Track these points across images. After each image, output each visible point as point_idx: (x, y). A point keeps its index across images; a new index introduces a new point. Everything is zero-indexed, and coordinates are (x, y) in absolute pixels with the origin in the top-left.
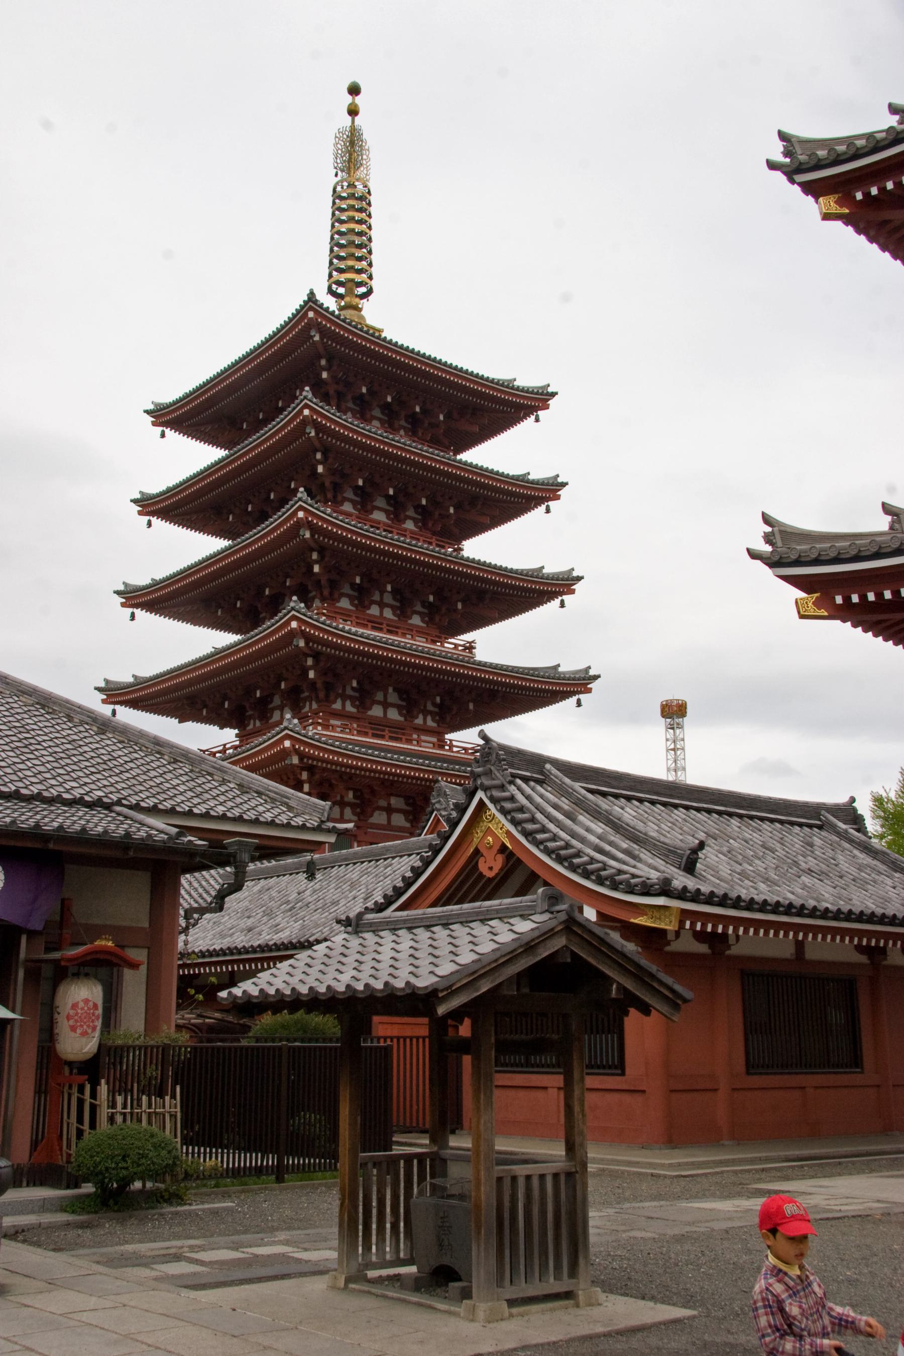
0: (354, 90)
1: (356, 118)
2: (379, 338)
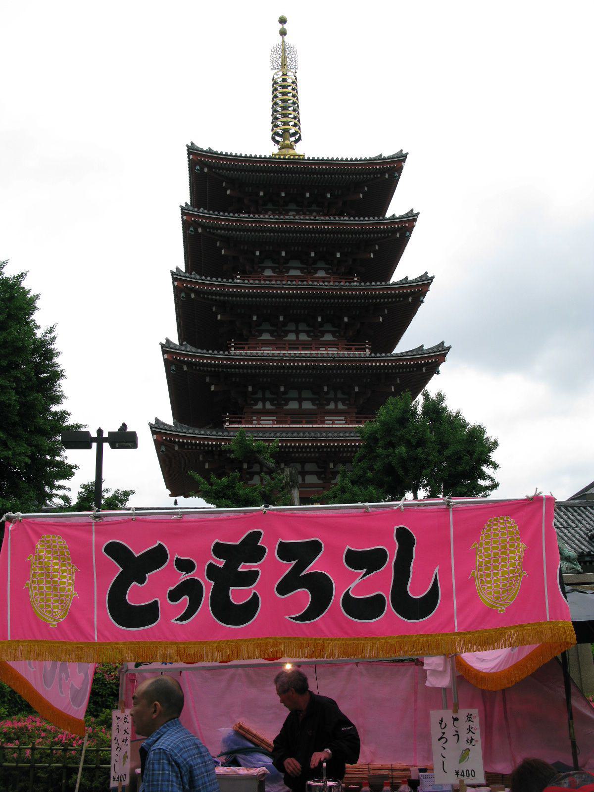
0: (283, 21)
1: (286, 37)
2: (304, 159)
